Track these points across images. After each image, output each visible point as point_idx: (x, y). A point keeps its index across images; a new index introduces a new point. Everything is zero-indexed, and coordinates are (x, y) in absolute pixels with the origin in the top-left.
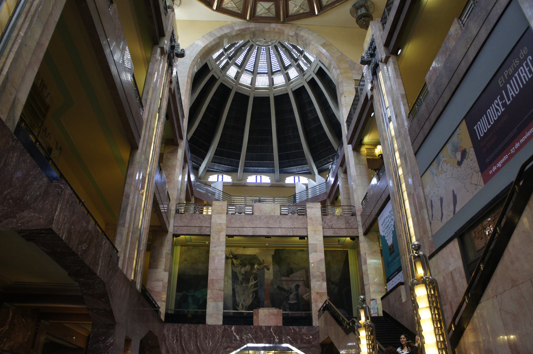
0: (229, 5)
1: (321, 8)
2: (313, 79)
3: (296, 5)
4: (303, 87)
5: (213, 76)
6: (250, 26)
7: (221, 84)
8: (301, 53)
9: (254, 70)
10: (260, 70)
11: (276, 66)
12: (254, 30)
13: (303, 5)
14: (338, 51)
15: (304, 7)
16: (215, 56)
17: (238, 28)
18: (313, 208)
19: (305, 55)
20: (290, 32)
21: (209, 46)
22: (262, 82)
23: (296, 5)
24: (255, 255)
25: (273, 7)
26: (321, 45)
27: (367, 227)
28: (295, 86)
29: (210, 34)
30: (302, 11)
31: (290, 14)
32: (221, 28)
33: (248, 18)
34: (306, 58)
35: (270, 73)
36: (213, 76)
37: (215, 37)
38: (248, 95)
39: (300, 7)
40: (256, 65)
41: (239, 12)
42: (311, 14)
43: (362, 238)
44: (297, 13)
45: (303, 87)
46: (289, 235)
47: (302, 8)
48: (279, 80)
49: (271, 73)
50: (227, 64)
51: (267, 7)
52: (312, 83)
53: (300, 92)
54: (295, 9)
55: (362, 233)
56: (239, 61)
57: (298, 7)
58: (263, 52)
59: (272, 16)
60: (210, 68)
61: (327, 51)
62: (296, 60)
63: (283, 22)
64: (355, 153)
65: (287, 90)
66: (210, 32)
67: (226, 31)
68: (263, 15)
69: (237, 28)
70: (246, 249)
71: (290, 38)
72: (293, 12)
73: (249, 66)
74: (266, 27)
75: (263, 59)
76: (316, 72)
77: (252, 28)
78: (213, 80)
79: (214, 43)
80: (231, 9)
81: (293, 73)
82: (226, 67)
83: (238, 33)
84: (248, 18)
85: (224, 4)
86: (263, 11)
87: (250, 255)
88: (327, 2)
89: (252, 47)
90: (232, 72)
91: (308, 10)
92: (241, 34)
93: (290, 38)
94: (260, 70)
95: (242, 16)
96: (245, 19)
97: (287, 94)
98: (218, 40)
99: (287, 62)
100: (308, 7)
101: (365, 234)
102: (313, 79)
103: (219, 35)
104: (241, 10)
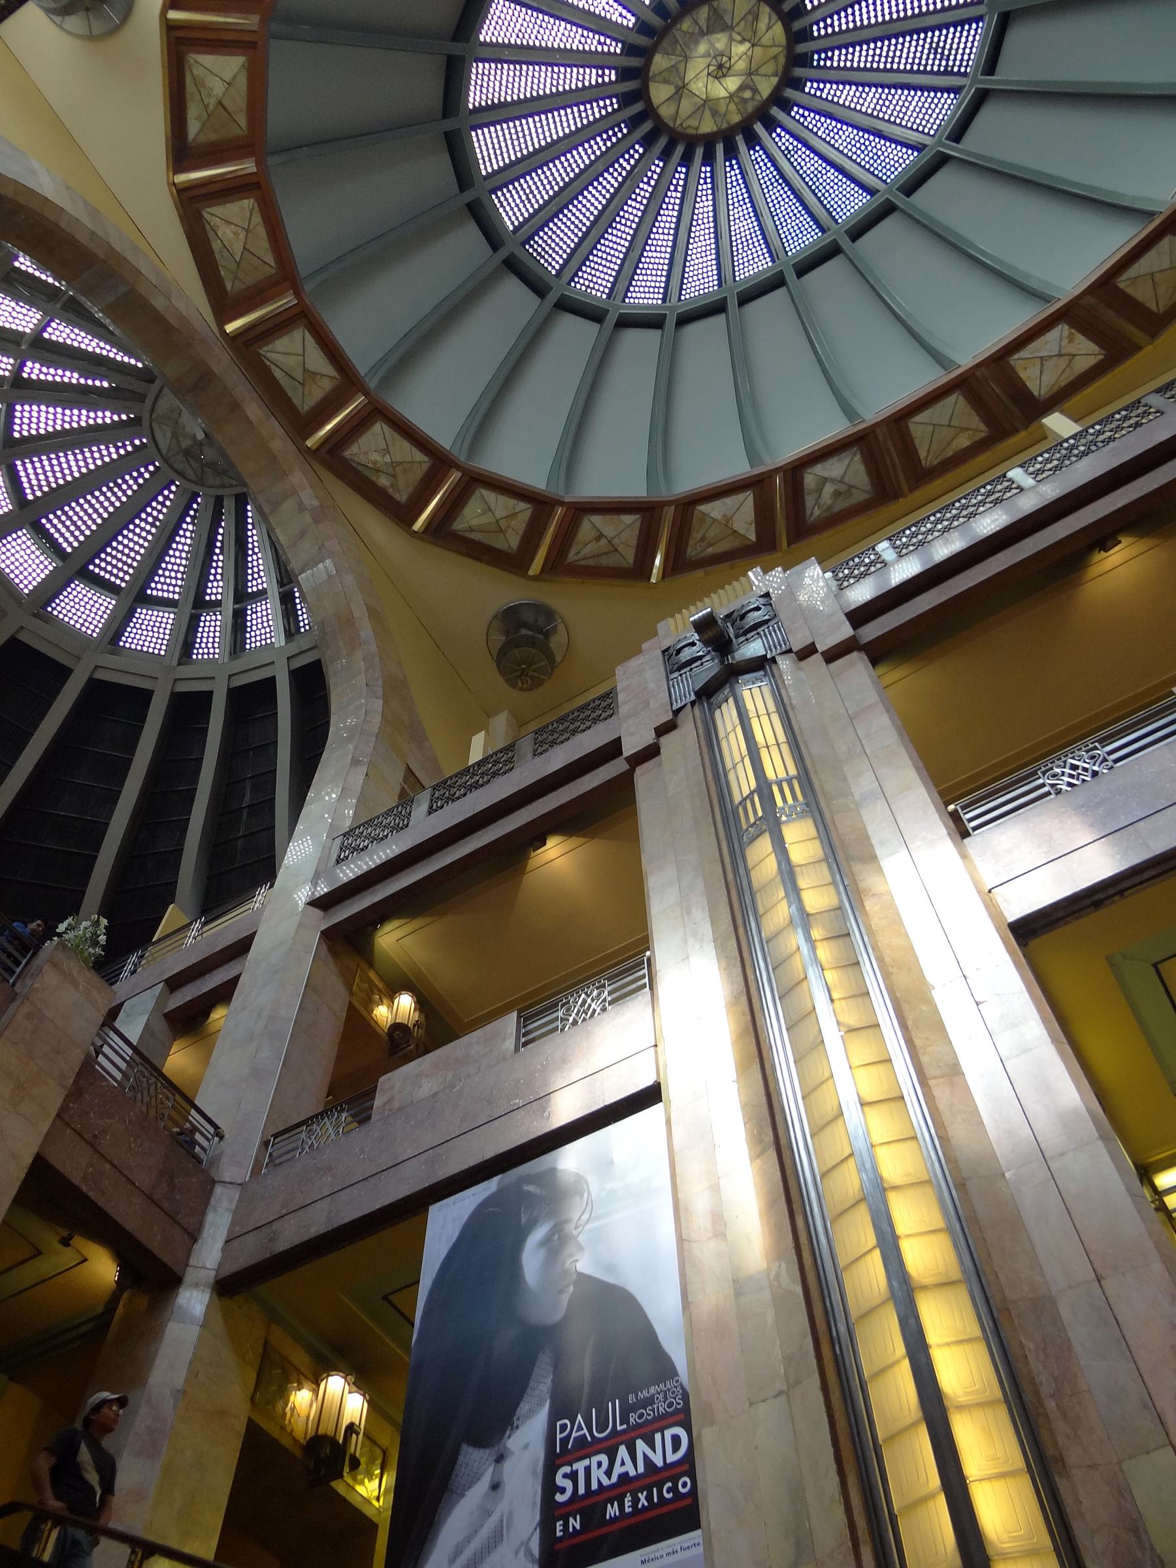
0: (226, 232)
1: (441, 532)
2: (209, 695)
3: (387, 451)
4: (147, 695)
8: (243, 597)
10: (54, 524)
12: (217, 369)
13: (405, 470)
15: (402, 481)
18: (75, 984)
20: (309, 491)
21: (63, 224)
23: (387, 451)
25: (326, 385)
30: (384, 481)
31: (347, 454)
33: (230, 328)
39: (395, 464)
41: (228, 285)
42: (402, 514)
43: (194, 1301)
44: (368, 473)
45: (147, 695)
47: (394, 476)
49: (77, 567)
51: (311, 366)
54: (375, 457)
57: (388, 459)
59: (297, 401)
62: (201, 604)
64: (324, 949)
68: (278, 374)
72: (362, 459)
74: (254, 410)
76: (238, 682)
79: (82, 238)
80: (216, 245)
81: (151, 633)
83: (170, 318)
84: (230, 328)
85: (216, 210)
86: (291, 362)
88: (472, 530)
91: (402, 496)
94: (54, 524)
96: (222, 320)
97: (65, 673)
100: (411, 489)
104: (239, 286)
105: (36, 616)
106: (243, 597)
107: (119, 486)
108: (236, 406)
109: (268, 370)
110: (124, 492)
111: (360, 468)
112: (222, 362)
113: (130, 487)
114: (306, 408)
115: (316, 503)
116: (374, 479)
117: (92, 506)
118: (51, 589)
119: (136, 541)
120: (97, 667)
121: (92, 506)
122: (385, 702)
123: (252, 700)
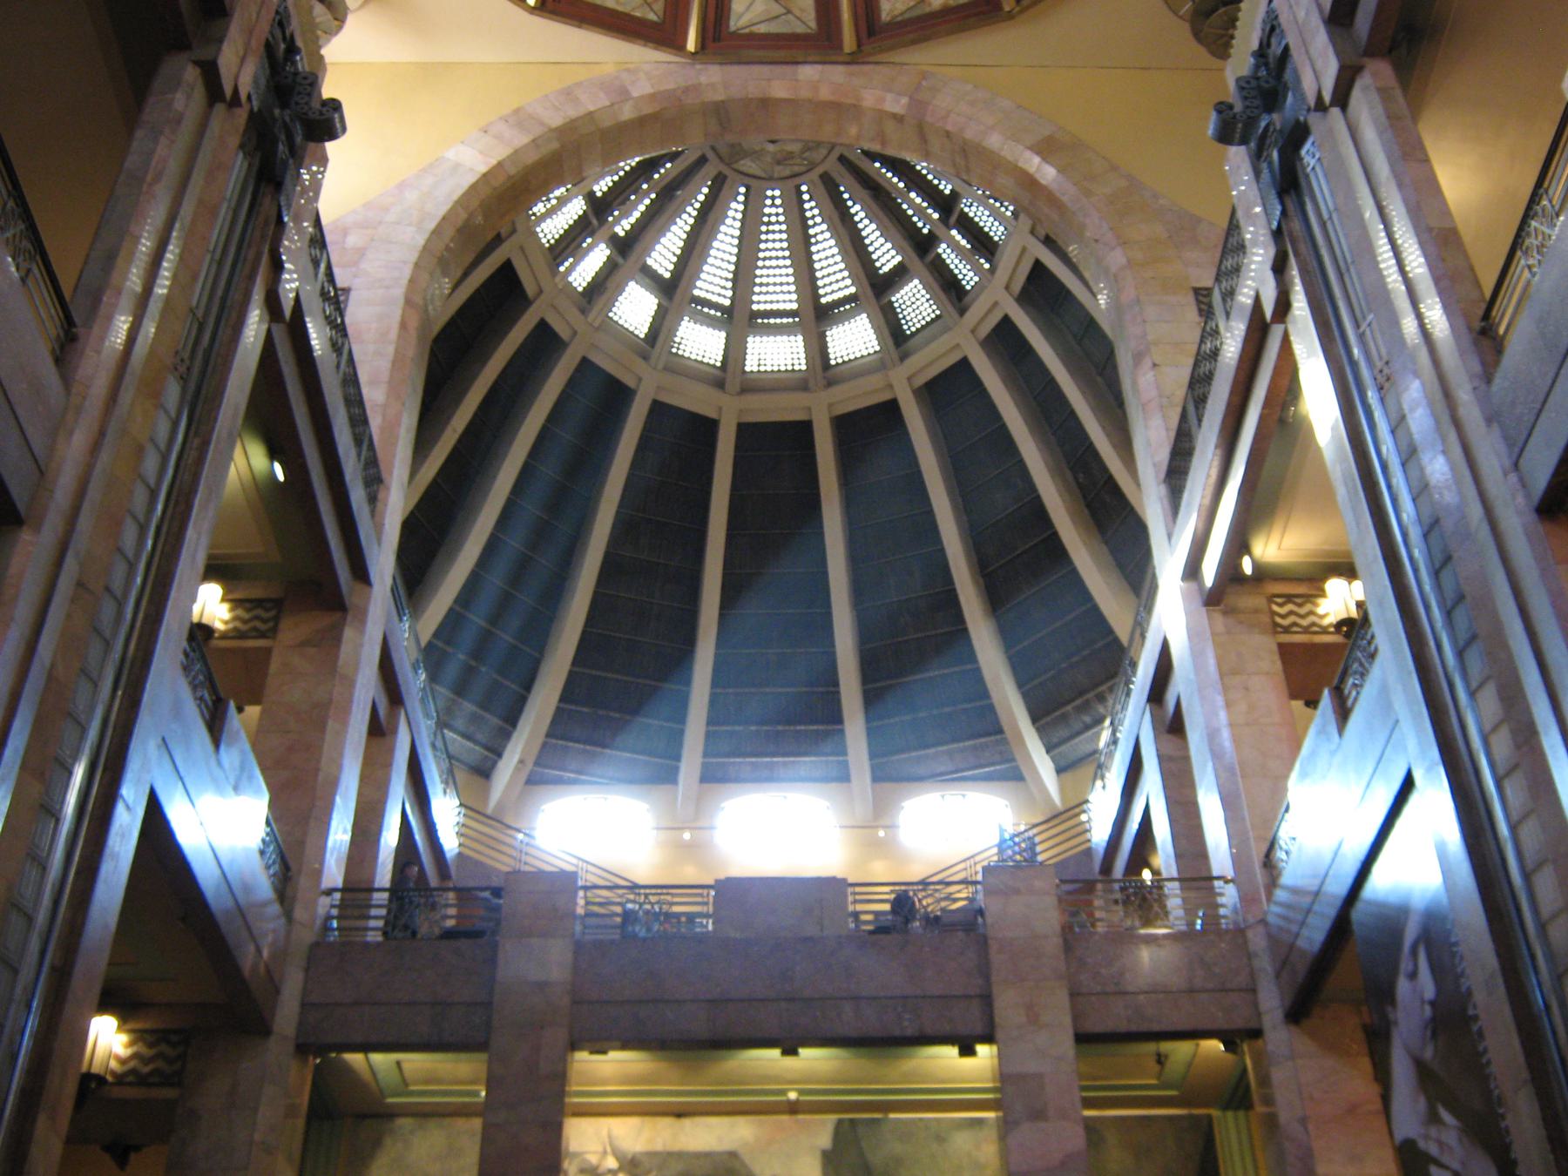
2: (1006, 321)
5: (543, 326)
6: (703, 79)
7: (585, 361)
8: (946, 205)
9: (733, 299)
11: (835, 281)
12: (719, 96)
14: (1114, 168)
16: (551, 229)
17: (648, 90)
19: (964, 215)
20: (889, 97)
21: (512, 171)
22: (777, 353)
24: (733, 1155)
26: (1031, 148)
27: (1300, 977)
28: (930, 361)
29: (518, 117)
32: (568, 93)
33: (691, 45)
34: (970, 228)
35: (810, 314)
36: (543, 326)
37: (538, 131)
38: (712, 414)
40: (743, 276)
41: (652, 17)
43: (1278, 1035)
45: (964, 364)
46: (897, 1033)
48: (854, 339)
50: (610, 268)
52: (1005, 340)
53: (952, 391)
55: (1279, 1014)
56: (663, 255)
58: (774, 207)
59: (800, 29)
60: (530, 288)
61: (1061, 170)
63: (854, 59)
65: (891, 386)
66: (517, 111)
67: (592, 102)
68: (762, 29)
69: (641, 88)
70: (687, 1123)
71: (890, 127)
73: (713, 282)
75: (775, 242)
76: (1018, 286)
77: (712, 85)
78: (545, 342)
79: (532, 157)
81: (915, 302)
82: (603, 287)
84: (691, 45)
87: (707, 1155)
89: (718, 185)
90: (635, 308)
92: (660, 119)
93: (890, 127)
95: (664, 34)
98: (555, 145)
99: (886, 256)
101: (1296, 1013)
102: (1006, 321)
103: (556, 121)
105: (830, 383)
106: (946, 205)
107: (769, 223)
108: (765, 103)
109: (752, 37)
110: (778, 222)
111: (907, 16)
112: (719, 80)
113: (777, 215)
114: (813, 24)
115: (904, 100)
116: (927, 10)
117: (770, 258)
118: (817, 350)
119: (827, 252)
120: (909, 379)
121: (770, 258)
122: (1124, 243)
123: (1041, 290)
